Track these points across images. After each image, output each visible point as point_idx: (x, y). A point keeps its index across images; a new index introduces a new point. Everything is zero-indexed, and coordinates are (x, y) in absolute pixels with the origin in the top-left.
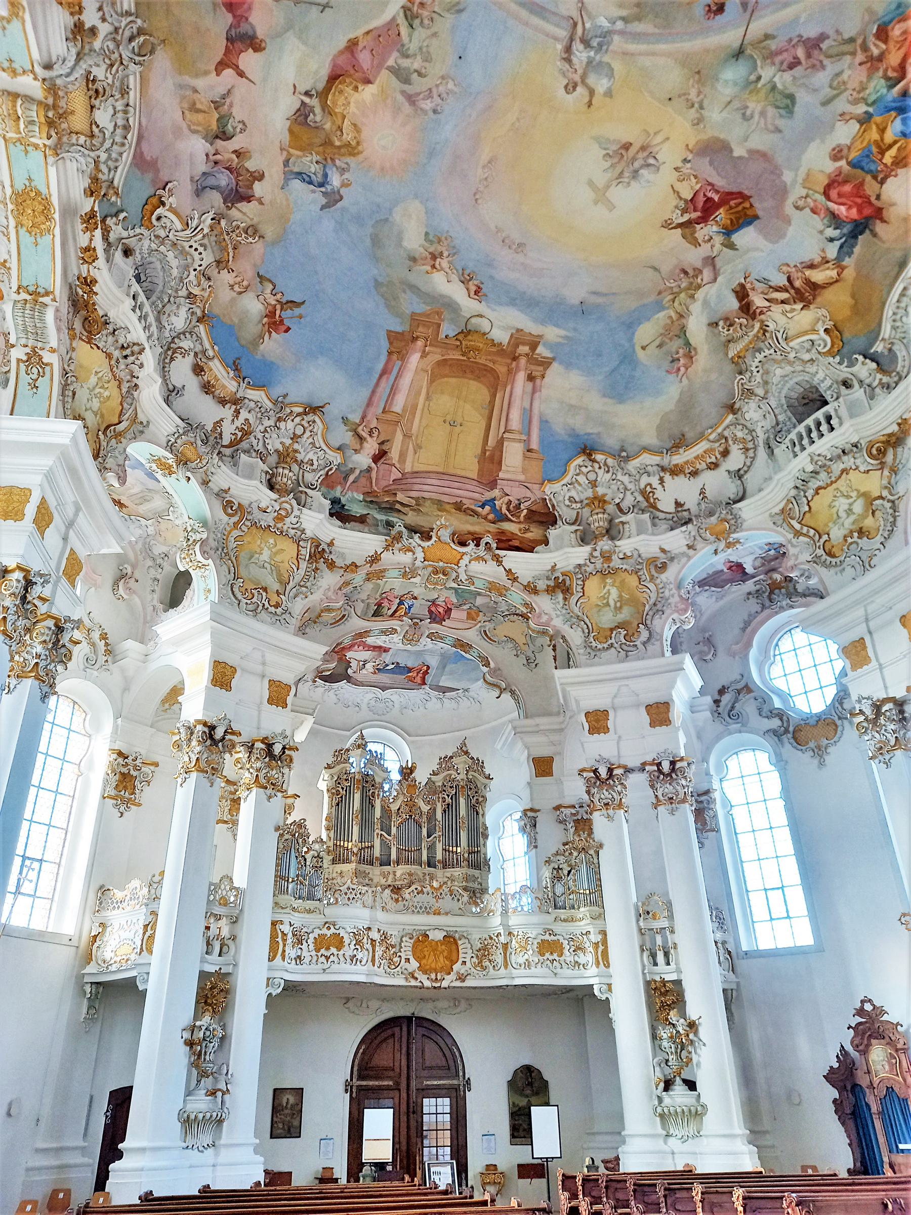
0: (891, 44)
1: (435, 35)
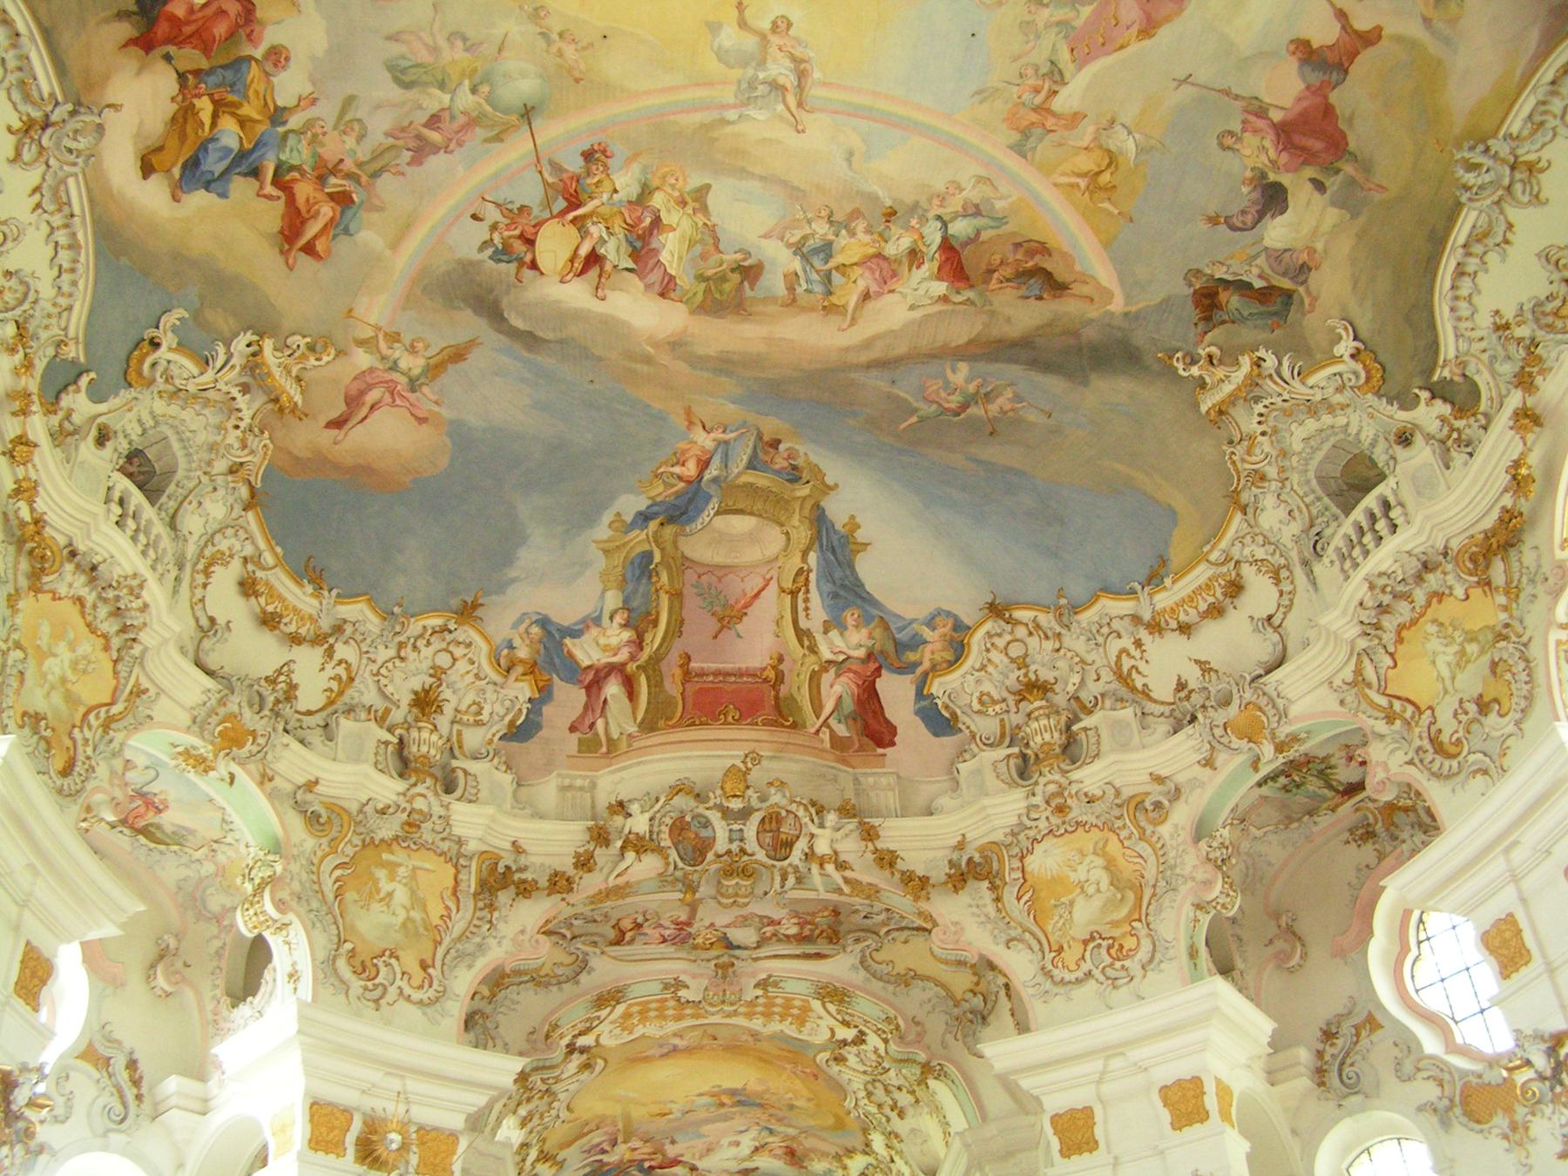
0: (320, 196)
1: (1016, 59)
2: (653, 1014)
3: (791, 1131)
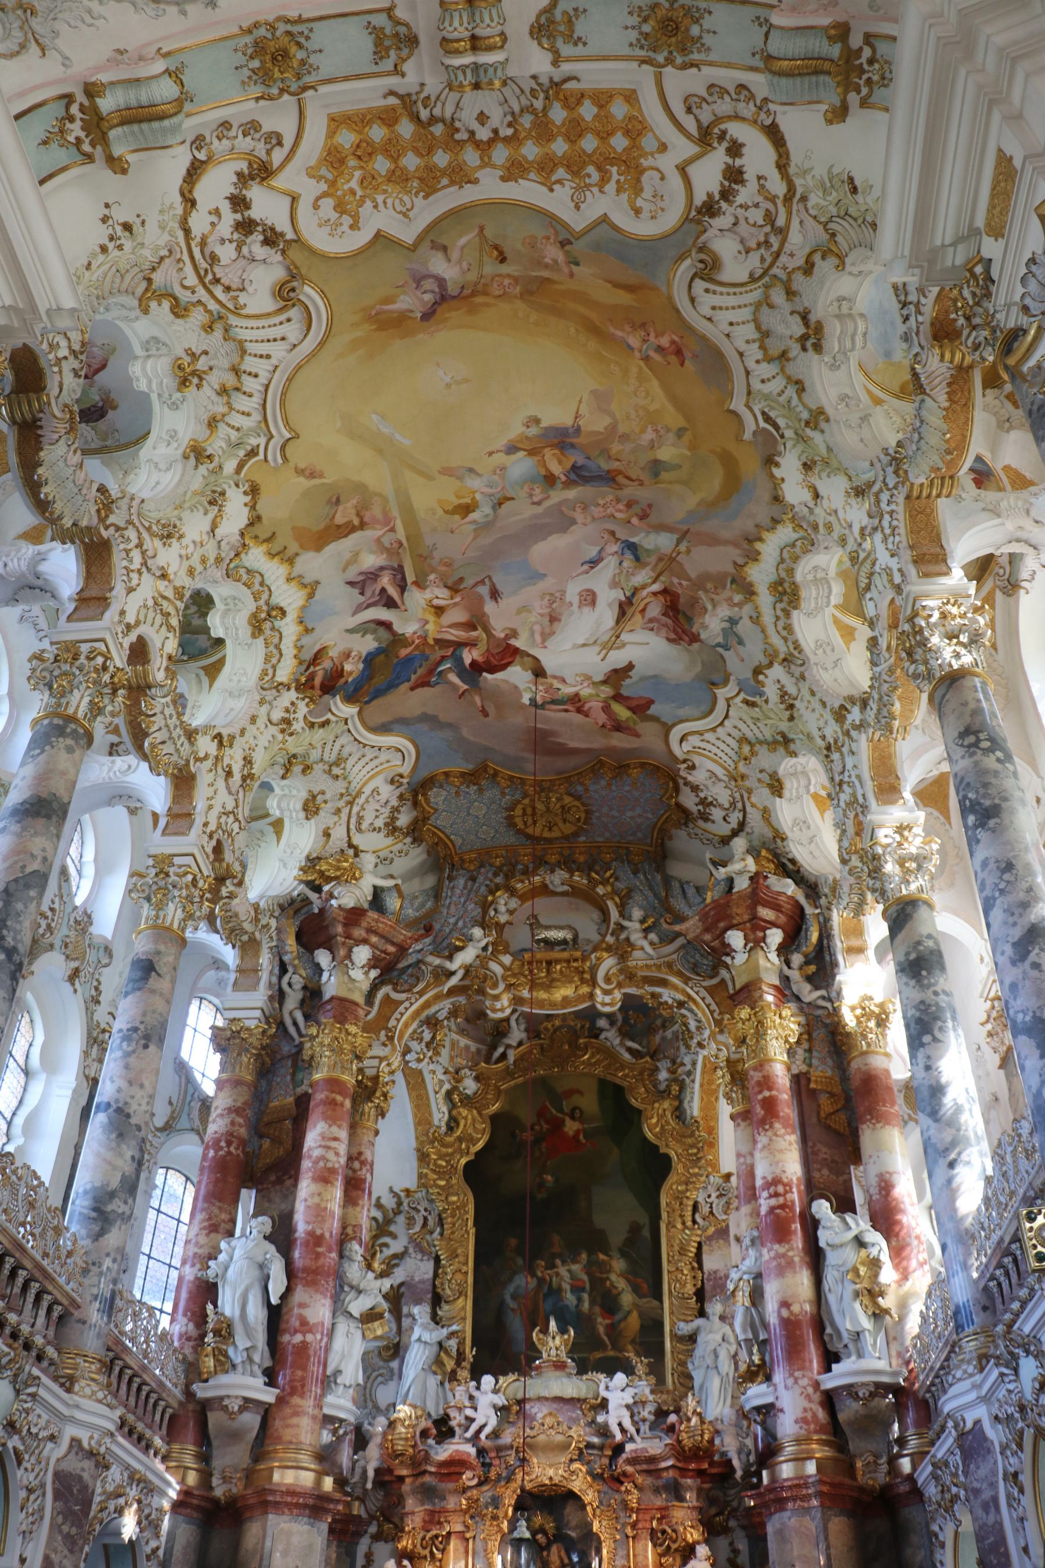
2: (381, 165)
3: (664, 542)
